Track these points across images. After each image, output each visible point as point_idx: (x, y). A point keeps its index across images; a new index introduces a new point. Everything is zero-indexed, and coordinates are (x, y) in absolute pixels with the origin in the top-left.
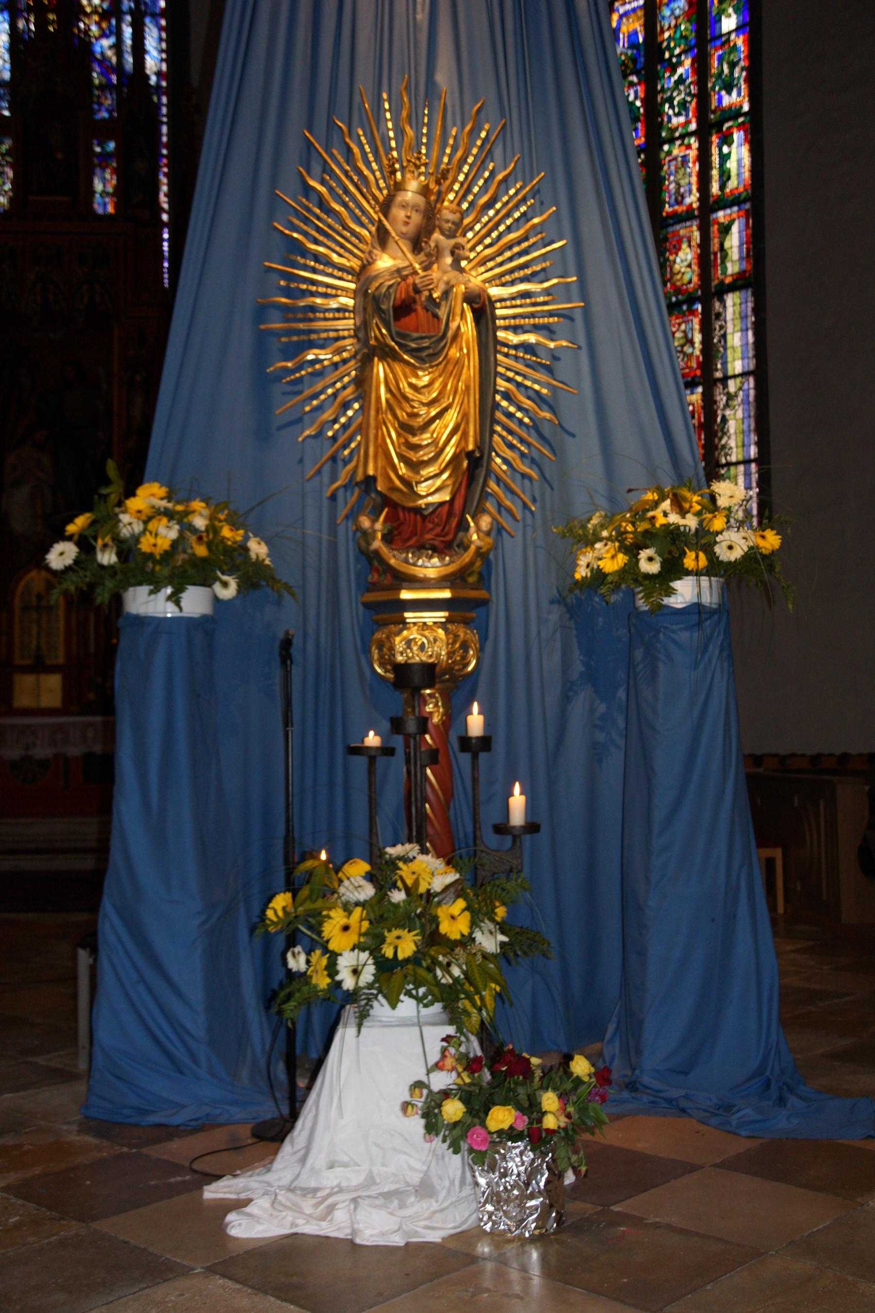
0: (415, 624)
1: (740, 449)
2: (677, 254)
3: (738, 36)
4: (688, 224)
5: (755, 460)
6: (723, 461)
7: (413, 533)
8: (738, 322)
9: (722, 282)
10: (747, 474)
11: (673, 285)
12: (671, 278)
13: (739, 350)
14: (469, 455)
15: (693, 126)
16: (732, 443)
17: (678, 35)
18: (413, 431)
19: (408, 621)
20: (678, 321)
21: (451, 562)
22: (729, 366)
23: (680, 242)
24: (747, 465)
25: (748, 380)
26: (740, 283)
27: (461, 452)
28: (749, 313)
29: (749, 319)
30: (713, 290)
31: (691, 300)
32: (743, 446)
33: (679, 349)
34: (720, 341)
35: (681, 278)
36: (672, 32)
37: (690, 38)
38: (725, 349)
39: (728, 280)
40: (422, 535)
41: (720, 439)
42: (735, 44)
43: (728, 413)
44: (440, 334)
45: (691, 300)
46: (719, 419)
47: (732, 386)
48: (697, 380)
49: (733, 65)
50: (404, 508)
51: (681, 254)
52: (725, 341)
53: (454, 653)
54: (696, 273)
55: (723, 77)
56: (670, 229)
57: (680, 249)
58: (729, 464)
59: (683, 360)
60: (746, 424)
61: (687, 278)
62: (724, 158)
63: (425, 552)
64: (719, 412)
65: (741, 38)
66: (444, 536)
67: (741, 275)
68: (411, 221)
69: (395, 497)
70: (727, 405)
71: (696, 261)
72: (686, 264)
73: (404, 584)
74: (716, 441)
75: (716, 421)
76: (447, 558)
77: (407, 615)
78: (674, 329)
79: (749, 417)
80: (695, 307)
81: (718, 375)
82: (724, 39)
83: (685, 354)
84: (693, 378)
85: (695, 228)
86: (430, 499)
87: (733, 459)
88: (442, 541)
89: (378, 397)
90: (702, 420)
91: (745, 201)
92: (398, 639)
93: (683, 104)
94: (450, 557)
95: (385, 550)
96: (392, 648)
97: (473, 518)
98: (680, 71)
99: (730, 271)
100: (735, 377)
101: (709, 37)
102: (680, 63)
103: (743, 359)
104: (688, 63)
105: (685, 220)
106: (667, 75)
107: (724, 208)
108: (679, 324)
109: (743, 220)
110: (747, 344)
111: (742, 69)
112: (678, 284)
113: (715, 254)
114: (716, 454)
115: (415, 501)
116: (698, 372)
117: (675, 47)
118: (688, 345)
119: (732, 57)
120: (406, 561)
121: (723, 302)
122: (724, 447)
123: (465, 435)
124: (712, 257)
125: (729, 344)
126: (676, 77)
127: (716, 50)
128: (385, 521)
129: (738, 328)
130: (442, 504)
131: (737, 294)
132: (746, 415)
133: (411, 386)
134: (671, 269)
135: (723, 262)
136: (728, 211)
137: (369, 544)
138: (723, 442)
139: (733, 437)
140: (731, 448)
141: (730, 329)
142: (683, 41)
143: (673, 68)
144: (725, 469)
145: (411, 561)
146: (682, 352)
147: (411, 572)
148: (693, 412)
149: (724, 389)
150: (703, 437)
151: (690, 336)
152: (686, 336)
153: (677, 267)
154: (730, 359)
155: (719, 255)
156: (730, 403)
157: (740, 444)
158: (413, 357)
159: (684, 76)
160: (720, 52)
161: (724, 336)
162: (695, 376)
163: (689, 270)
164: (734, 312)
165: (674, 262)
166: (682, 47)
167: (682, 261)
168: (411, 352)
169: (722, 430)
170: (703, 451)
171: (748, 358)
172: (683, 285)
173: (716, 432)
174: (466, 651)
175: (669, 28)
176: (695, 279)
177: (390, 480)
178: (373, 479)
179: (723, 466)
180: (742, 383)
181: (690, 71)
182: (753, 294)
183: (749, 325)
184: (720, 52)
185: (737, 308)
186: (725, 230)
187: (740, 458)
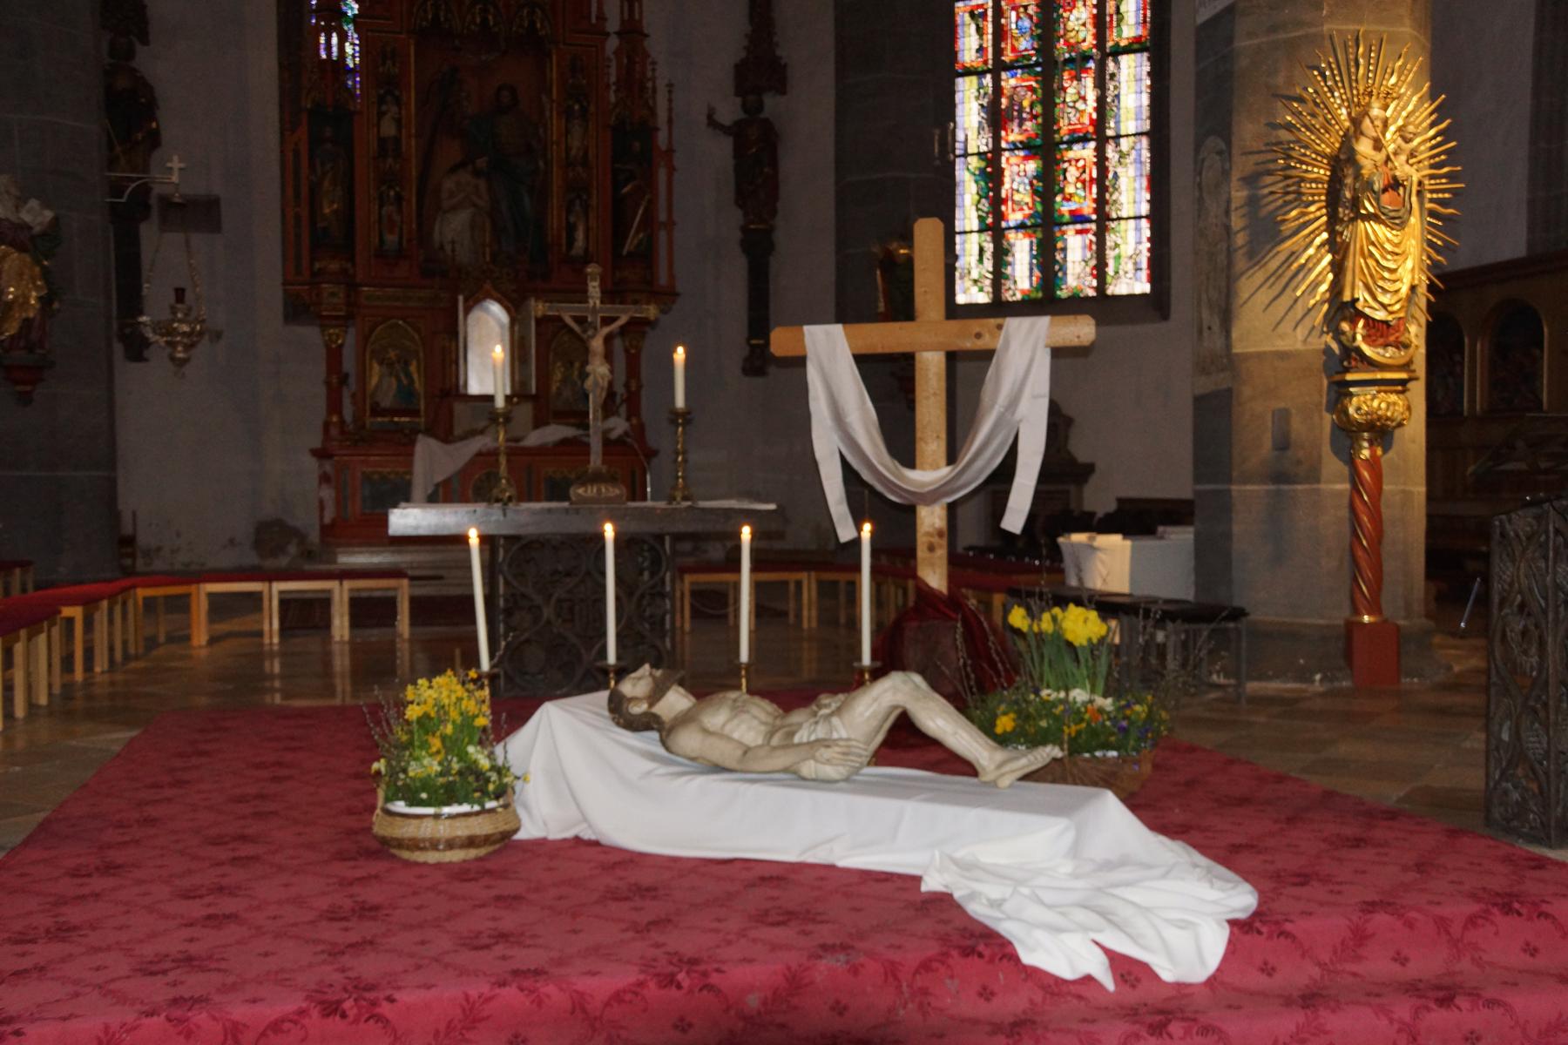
1: (1131, 205)
2: (1071, 11)
5: (1146, 217)
8: (1133, 84)
9: (1117, 44)
10: (1138, 229)
12: (1065, 34)
24: (1138, 221)
25: (1140, 141)
26: (1136, 46)
29: (1144, 82)
30: (1108, 51)
32: (1135, 202)
34: (1113, 101)
38: (1119, 109)
39: (1123, 43)
41: (1111, 195)
43: (1120, 170)
45: (1086, 58)
46: (1111, 176)
47: (1125, 144)
48: (1089, 136)
51: (1075, 12)
54: (1091, 33)
57: (1074, 7)
58: (1119, 219)
61: (1081, 36)
67: (1137, 39)
72: (1081, 22)
74: (1107, 196)
79: (1141, 175)
83: (1077, 110)
84: (1085, 134)
103: (1137, 120)
110: (1141, 106)
112: (1072, 41)
113: (1111, 16)
114: (1107, 209)
116: (1091, 129)
118: (1081, 101)
121: (1117, 62)
122: (1115, 201)
124: (1108, 19)
129: (1133, 89)
131: (1132, 56)
132: (1138, 173)
134: (1065, 25)
135: (1119, 25)
138: (1114, 197)
141: (1123, 91)
144: (1116, 223)
146: (1074, 107)
148: (1084, 167)
152: (1079, 93)
153: (1070, 25)
154: (1123, 118)
155: (1115, 17)
157: (1132, 201)
161: (1118, 96)
162: (1088, 132)
163: (1083, 28)
165: (1068, 19)
169: (1113, 186)
170: (1094, 205)
171: (1142, 119)
179: (1113, 220)
180: (1135, 143)
182: (1149, 59)
183: (1144, 88)
185: (1132, 70)
187: (1132, 215)
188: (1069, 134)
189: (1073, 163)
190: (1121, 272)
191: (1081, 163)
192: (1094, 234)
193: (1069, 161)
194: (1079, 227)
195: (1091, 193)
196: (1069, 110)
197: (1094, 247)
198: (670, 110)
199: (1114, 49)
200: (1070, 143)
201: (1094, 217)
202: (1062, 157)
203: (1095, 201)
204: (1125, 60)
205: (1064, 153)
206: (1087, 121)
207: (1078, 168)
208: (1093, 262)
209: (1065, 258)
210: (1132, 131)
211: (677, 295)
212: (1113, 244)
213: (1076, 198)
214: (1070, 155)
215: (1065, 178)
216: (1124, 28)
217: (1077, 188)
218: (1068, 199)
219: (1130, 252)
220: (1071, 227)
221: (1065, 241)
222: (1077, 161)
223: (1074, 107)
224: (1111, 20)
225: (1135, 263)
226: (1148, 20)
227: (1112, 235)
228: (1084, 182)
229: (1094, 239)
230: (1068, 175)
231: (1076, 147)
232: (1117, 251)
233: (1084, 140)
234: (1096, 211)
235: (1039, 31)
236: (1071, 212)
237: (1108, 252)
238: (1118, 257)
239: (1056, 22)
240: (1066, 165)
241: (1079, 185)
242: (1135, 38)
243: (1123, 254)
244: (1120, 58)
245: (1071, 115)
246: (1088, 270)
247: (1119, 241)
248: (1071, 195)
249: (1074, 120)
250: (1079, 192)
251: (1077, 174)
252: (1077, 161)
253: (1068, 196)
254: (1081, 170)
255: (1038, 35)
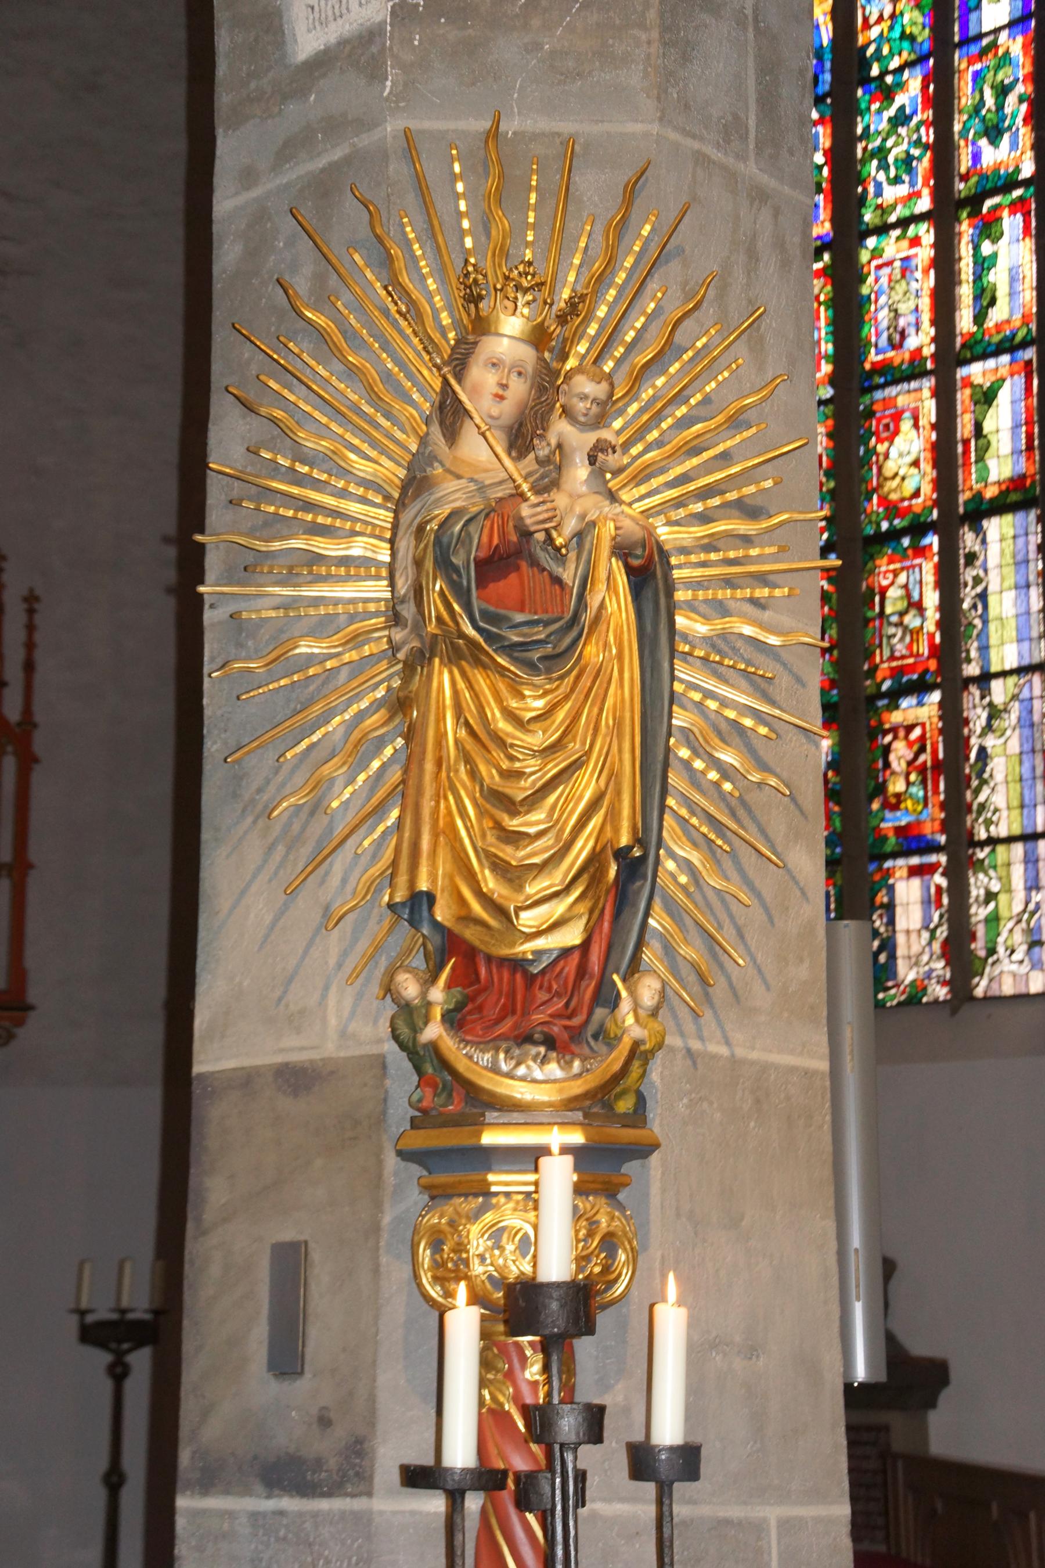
0: (507, 1195)
1: (1016, 813)
2: (891, 440)
3: (1012, 37)
4: (914, 385)
6: (983, 835)
7: (508, 1010)
8: (1010, 572)
9: (979, 496)
11: (884, 501)
12: (880, 486)
13: (1013, 623)
14: (621, 854)
15: (924, 204)
16: (999, 800)
17: (896, 34)
18: (513, 807)
19: (494, 1189)
20: (892, 567)
21: (585, 1071)
22: (994, 654)
23: (897, 417)
24: (1030, 845)
25: (1030, 681)
26: (1014, 497)
27: (604, 848)
28: (1032, 554)
29: (1032, 565)
30: (961, 510)
31: (918, 529)
32: (1022, 806)
33: (894, 619)
34: (974, 607)
35: (899, 486)
36: (885, 25)
37: (920, 39)
38: (985, 622)
39: (990, 493)
40: (526, 1013)
41: (977, 792)
42: (1007, 52)
43: (990, 742)
44: (568, 616)
45: (918, 529)
47: (999, 691)
49: (1002, 91)
50: (489, 959)
51: (898, 440)
52: (986, 607)
53: (587, 1258)
54: (928, 478)
55: (984, 112)
56: (879, 395)
57: (897, 432)
58: (992, 842)
59: (902, 639)
60: (1027, 765)
61: (909, 487)
62: (983, 265)
63: (533, 1050)
64: (973, 741)
65: (1020, 40)
66: (570, 1017)
67: (1017, 482)
68: (507, 394)
69: (470, 934)
70: (989, 728)
71: (929, 455)
72: (910, 459)
73: (491, 1116)
74: (969, 795)
75: (968, 758)
76: (577, 1064)
77: (491, 1177)
78: (885, 583)
79: (1033, 751)
80: (926, 541)
81: (972, 670)
82: (985, 42)
83: (906, 629)
85: (926, 393)
86: (540, 943)
87: (1002, 831)
88: (566, 1027)
89: (441, 736)
90: (941, 756)
91: (1024, 345)
92: (475, 1229)
93: (908, 161)
94: (584, 1059)
95: (449, 1045)
96: (460, 1248)
97: (624, 980)
98: (901, 99)
99: (993, 477)
100: (1004, 674)
101: (957, 39)
102: (901, 86)
103: (1019, 640)
104: (914, 82)
105: (909, 378)
106: (875, 106)
107: (984, 356)
108: (896, 573)
109: (1020, 380)
110: (1028, 613)
111: (1021, 100)
112: (894, 497)
113: (966, 443)
114: (969, 820)
115: (513, 944)
116: (933, 665)
117: (892, 54)
118: (913, 612)
119: (1000, 76)
120: (495, 1069)
121: (978, 530)
122: (982, 807)
123: (613, 815)
124: (960, 449)
125: (993, 611)
126: (892, 112)
127: (970, 63)
128: (449, 986)
129: (1010, 581)
130: (566, 952)
131: (1008, 519)
132: (1027, 747)
133: (511, 716)
134: (880, 469)
135: (980, 459)
136: (991, 363)
137: (416, 1030)
138: (982, 798)
139: (1001, 789)
140: (996, 810)
141: (994, 582)
142: (906, 45)
143: (887, 95)
145: (504, 1067)
146: (900, 624)
147: (501, 1090)
148: (922, 738)
149: (983, 697)
150: (942, 786)
151: (916, 596)
152: (908, 595)
153: (890, 467)
154: (994, 640)
156: (996, 724)
157: (1015, 803)
158: (515, 660)
159: (908, 111)
160: (978, 66)
161: (983, 596)
163: (914, 471)
164: (1002, 553)
166: (905, 55)
167: (901, 455)
168: (511, 650)
171: (1031, 639)
172: (903, 500)
173: (969, 778)
174: (612, 1255)
175: (880, 19)
176: (927, 489)
177: (462, 901)
178: (430, 898)
179: (982, 844)
181: (920, 100)
182: (1040, 519)
183: (1032, 577)
184: (978, 66)
186: (987, 397)
187: (1016, 830)
188: (892, 677)
189: (902, 733)
190: (1001, 950)
191: (917, 733)
192: (943, 874)
193: (894, 730)
194: (915, 861)
195: (936, 791)
196: (892, 630)
197: (945, 900)
198: (30, 646)
199: (971, 506)
200: (895, 696)
201: (943, 839)
202: (881, 723)
203: (943, 806)
204: (998, 527)
205: (885, 716)
206: (924, 649)
207: (910, 745)
208: (942, 933)
209: (891, 922)
210: (1011, 662)
211: (30, 1008)
212: (982, 892)
213: (909, 803)
214: (896, 717)
215: (887, 765)
216: (992, 463)
217: (908, 784)
218: (894, 804)
219: (1018, 907)
220: (901, 862)
221: (891, 889)
222: (910, 728)
223: (900, 624)
224: (966, 451)
225: (1029, 931)
226: (1036, 443)
227: (981, 876)
228: (922, 770)
229: (943, 882)
230: (892, 757)
231: (905, 703)
232: (992, 905)
233: (921, 688)
234: (945, 827)
235: (832, 484)
236: (899, 831)
237: (973, 910)
238: (993, 920)
239: (865, 463)
240: (888, 738)
241: (913, 777)
242: (1012, 480)
243: (1004, 912)
244: (985, 523)
245: (895, 640)
246: (937, 946)
247: (995, 887)
248: (898, 796)
249: (900, 649)
250: (913, 790)
251: (910, 756)
252: (910, 728)
253: (893, 801)
254: (916, 747)
255: (831, 492)
